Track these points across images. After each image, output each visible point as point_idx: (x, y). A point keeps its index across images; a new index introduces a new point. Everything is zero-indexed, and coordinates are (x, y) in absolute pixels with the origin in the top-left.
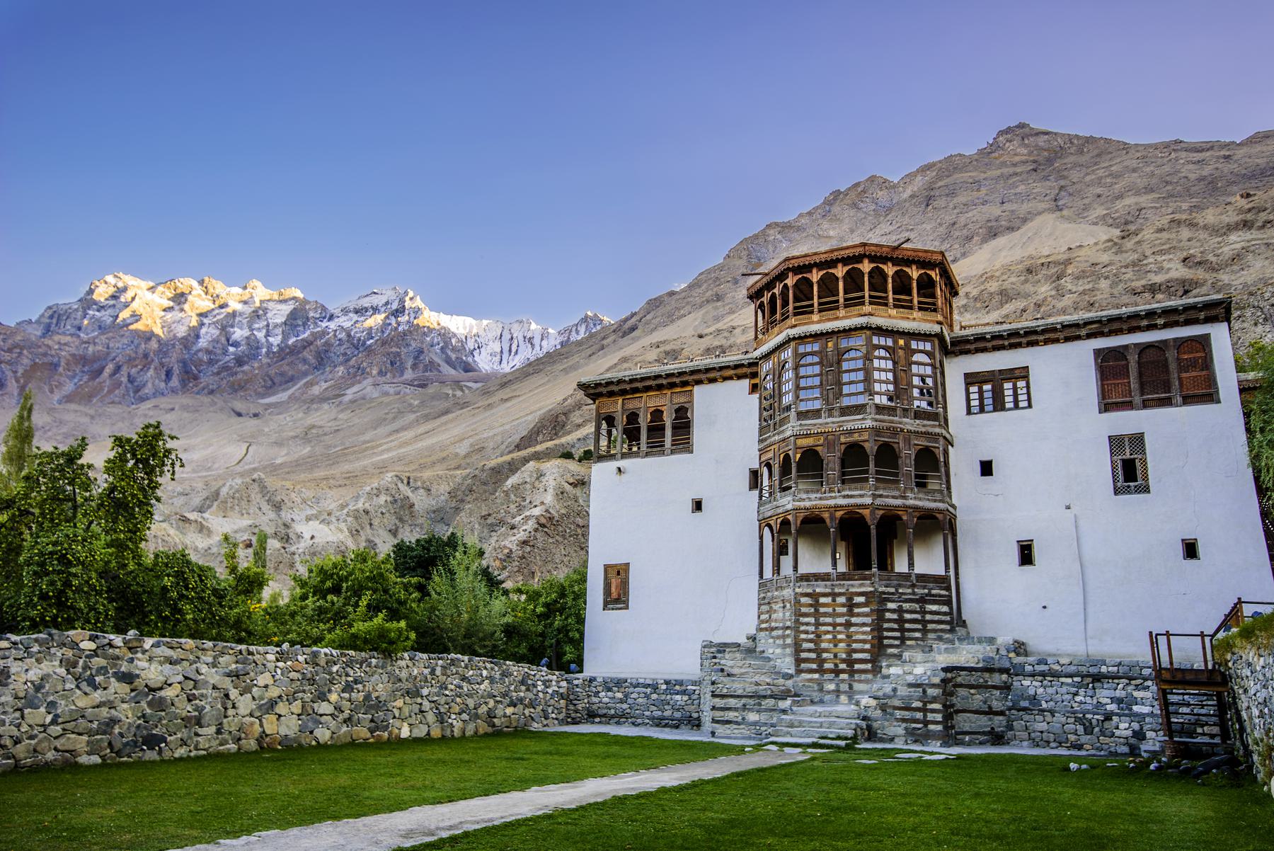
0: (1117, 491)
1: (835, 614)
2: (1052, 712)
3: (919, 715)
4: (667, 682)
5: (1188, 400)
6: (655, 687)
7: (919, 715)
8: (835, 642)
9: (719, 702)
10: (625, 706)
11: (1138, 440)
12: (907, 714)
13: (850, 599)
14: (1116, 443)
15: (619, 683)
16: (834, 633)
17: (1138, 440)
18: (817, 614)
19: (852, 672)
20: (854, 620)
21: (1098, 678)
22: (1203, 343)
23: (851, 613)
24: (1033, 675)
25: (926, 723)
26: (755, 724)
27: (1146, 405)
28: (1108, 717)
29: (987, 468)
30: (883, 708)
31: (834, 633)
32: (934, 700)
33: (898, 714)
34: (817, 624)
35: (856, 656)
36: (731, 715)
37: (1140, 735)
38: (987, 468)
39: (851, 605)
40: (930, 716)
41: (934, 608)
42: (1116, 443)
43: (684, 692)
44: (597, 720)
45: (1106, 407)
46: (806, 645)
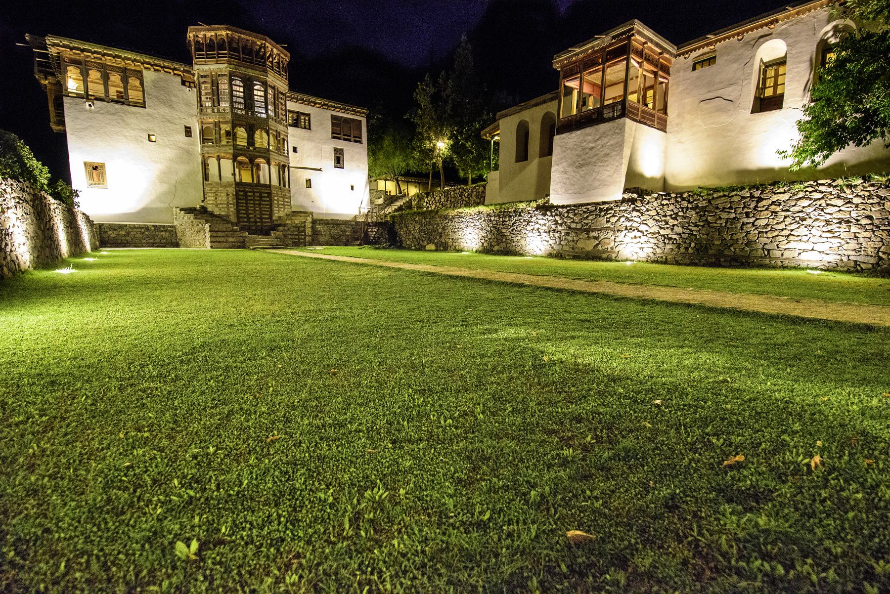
1: (254, 200)
4: (154, 226)
6: (147, 228)
8: (255, 211)
9: (215, 234)
10: (128, 238)
11: (341, 151)
15: (121, 227)
16: (255, 208)
17: (341, 151)
18: (246, 200)
22: (360, 121)
25: (299, 239)
27: (345, 139)
28: (340, 236)
29: (295, 150)
30: (284, 235)
31: (255, 208)
34: (247, 203)
37: (347, 241)
38: (295, 150)
39: (261, 197)
42: (336, 150)
43: (166, 231)
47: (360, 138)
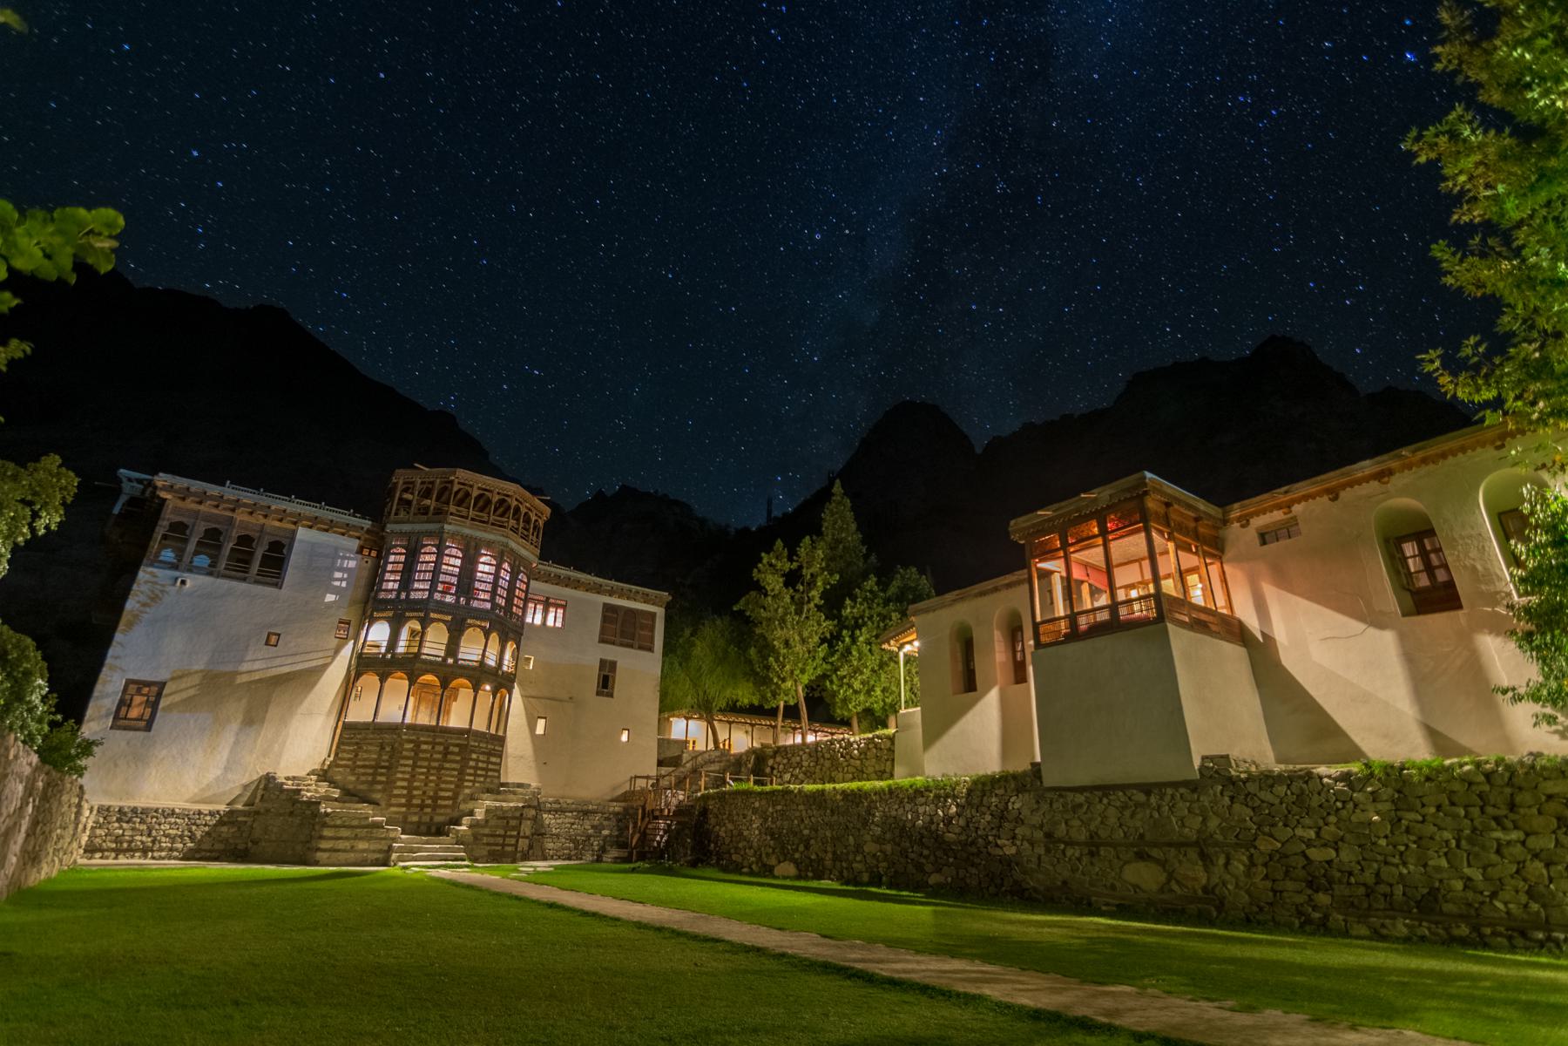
0: (598, 694)
1: (431, 759)
2: (558, 836)
3: (500, 840)
5: (641, 648)
7: (500, 840)
11: (613, 665)
12: (492, 840)
13: (446, 748)
14: (603, 663)
16: (427, 774)
17: (613, 665)
19: (435, 807)
20: (447, 765)
21: (586, 813)
23: (445, 759)
24: (549, 812)
25: (503, 845)
26: (364, 851)
27: (622, 645)
28: (589, 837)
31: (427, 774)
32: (513, 828)
33: (485, 840)
34: (414, 766)
35: (442, 794)
36: (341, 845)
39: (446, 753)
40: (508, 841)
41: (493, 759)
42: (603, 663)
44: (98, 855)
45: (602, 641)
46: (400, 784)
47: (652, 642)
